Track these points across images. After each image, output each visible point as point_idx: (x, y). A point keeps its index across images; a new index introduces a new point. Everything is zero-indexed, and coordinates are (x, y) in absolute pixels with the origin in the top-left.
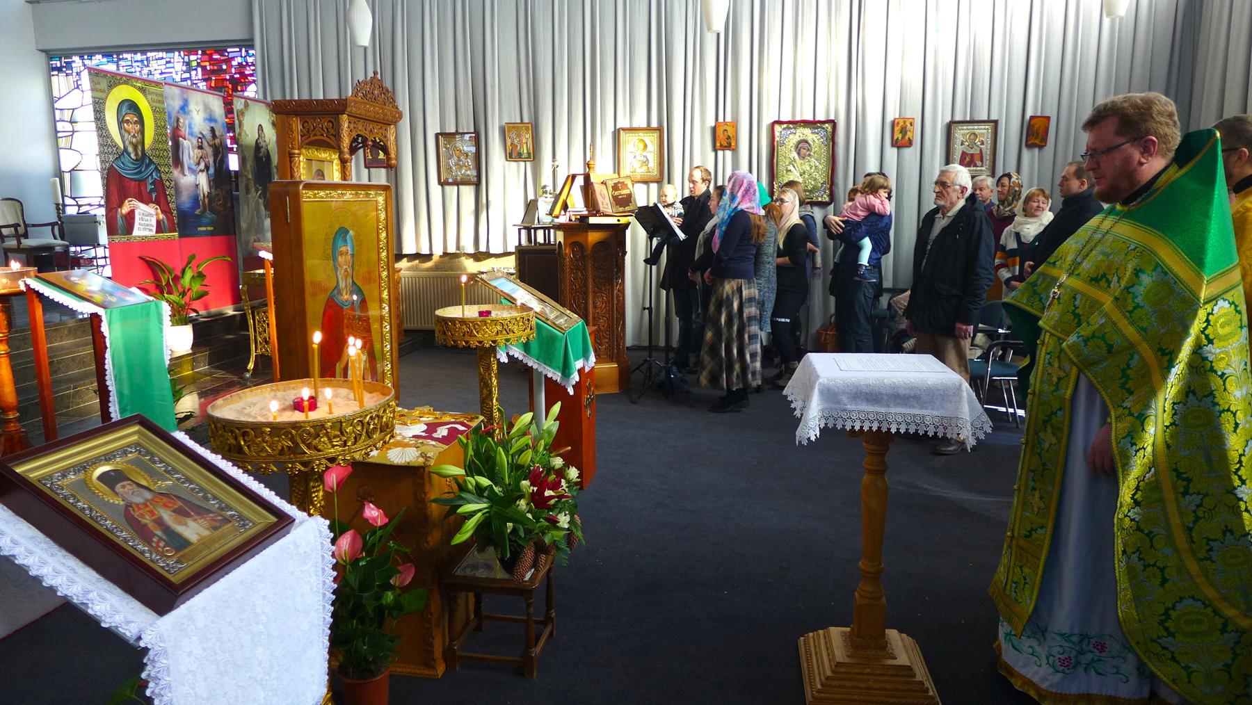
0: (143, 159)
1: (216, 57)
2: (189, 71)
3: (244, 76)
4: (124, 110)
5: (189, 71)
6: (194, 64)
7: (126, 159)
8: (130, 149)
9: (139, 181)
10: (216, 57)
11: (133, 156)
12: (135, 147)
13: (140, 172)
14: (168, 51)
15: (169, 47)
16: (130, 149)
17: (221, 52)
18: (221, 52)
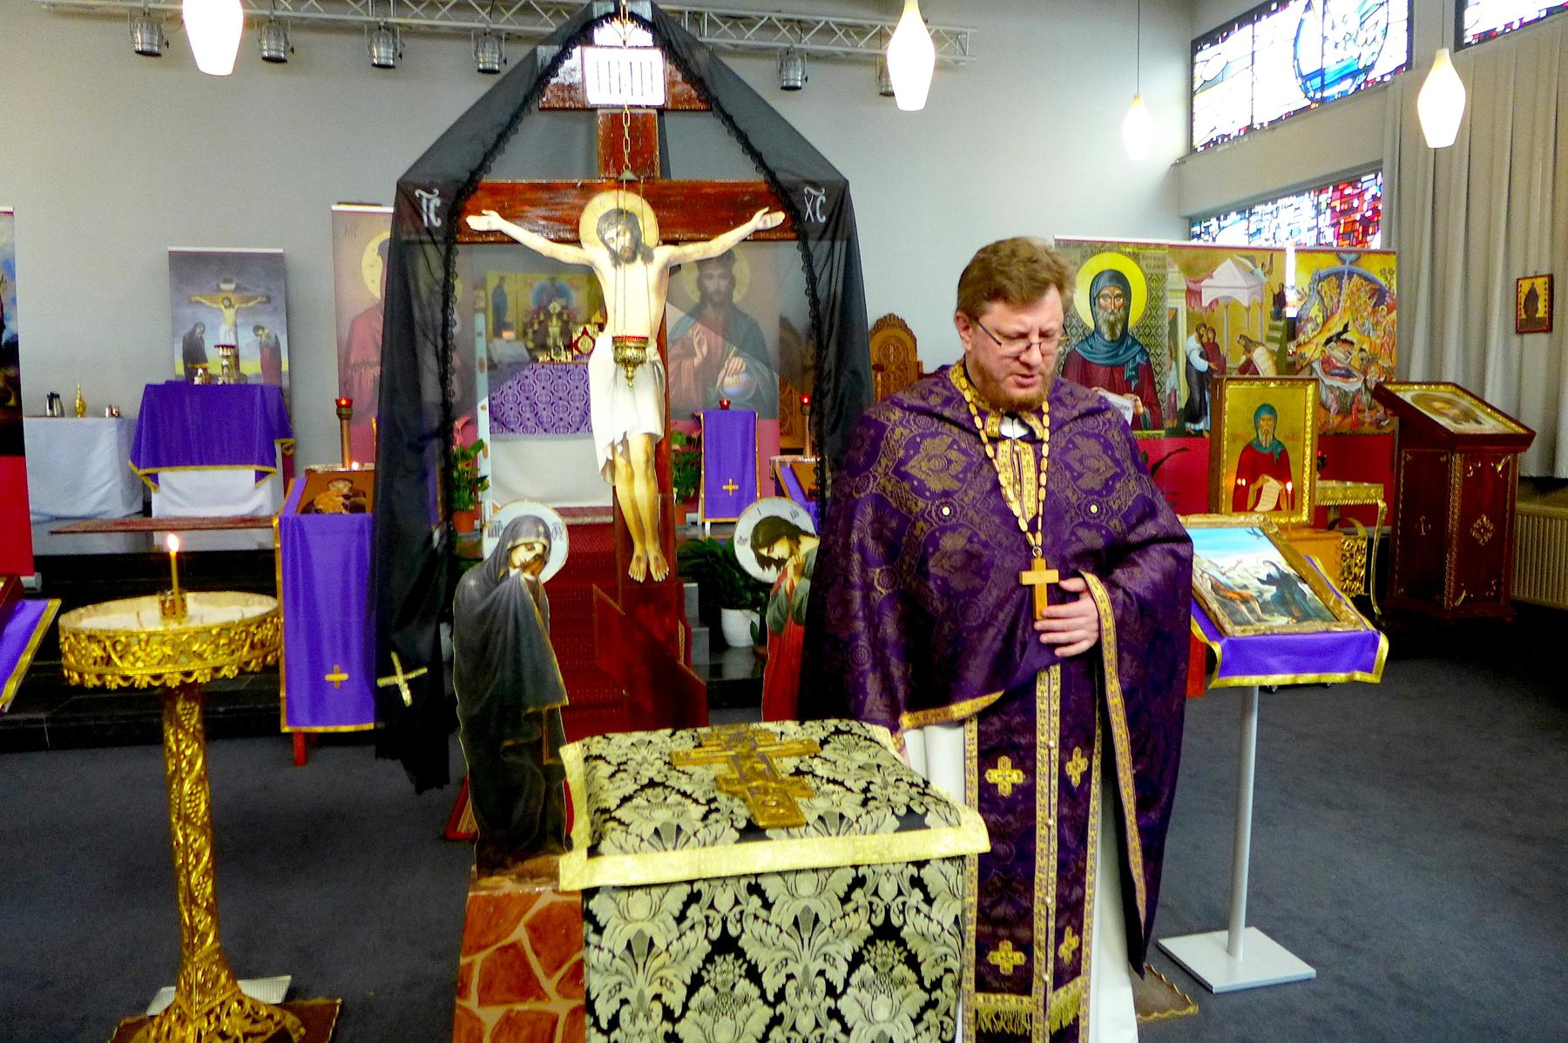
0: (1123, 338)
1: (1348, 191)
2: (1319, 213)
3: (1376, 211)
4: (1101, 285)
5: (1319, 213)
6: (1323, 206)
7: (1098, 343)
8: (1105, 329)
9: (1112, 366)
10: (1348, 191)
11: (1107, 337)
12: (1112, 326)
13: (1116, 355)
14: (1299, 193)
15: (1298, 191)
16: (1105, 329)
17: (1353, 183)
18: (1353, 183)
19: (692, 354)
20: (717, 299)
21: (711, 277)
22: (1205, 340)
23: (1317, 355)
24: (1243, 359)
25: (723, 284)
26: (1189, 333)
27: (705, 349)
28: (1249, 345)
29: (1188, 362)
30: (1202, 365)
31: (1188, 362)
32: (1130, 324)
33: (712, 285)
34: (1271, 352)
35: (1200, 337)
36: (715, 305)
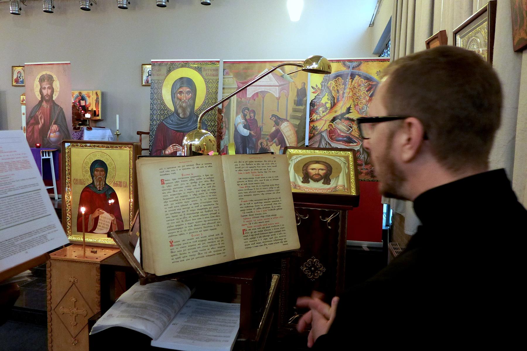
19: (38, 123)
20: (47, 98)
21: (45, 88)
22: (248, 117)
23: (326, 127)
24: (274, 129)
25: (49, 91)
26: (237, 114)
27: (43, 121)
28: (278, 121)
29: (236, 131)
30: (246, 132)
31: (236, 131)
32: (196, 107)
33: (45, 92)
34: (294, 126)
35: (245, 116)
36: (47, 101)
